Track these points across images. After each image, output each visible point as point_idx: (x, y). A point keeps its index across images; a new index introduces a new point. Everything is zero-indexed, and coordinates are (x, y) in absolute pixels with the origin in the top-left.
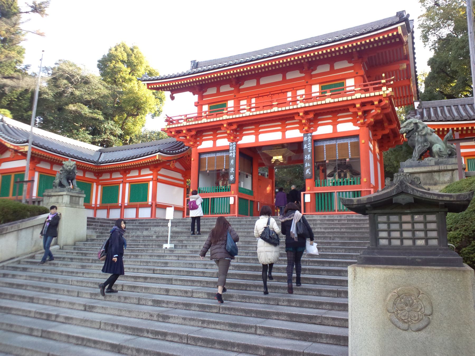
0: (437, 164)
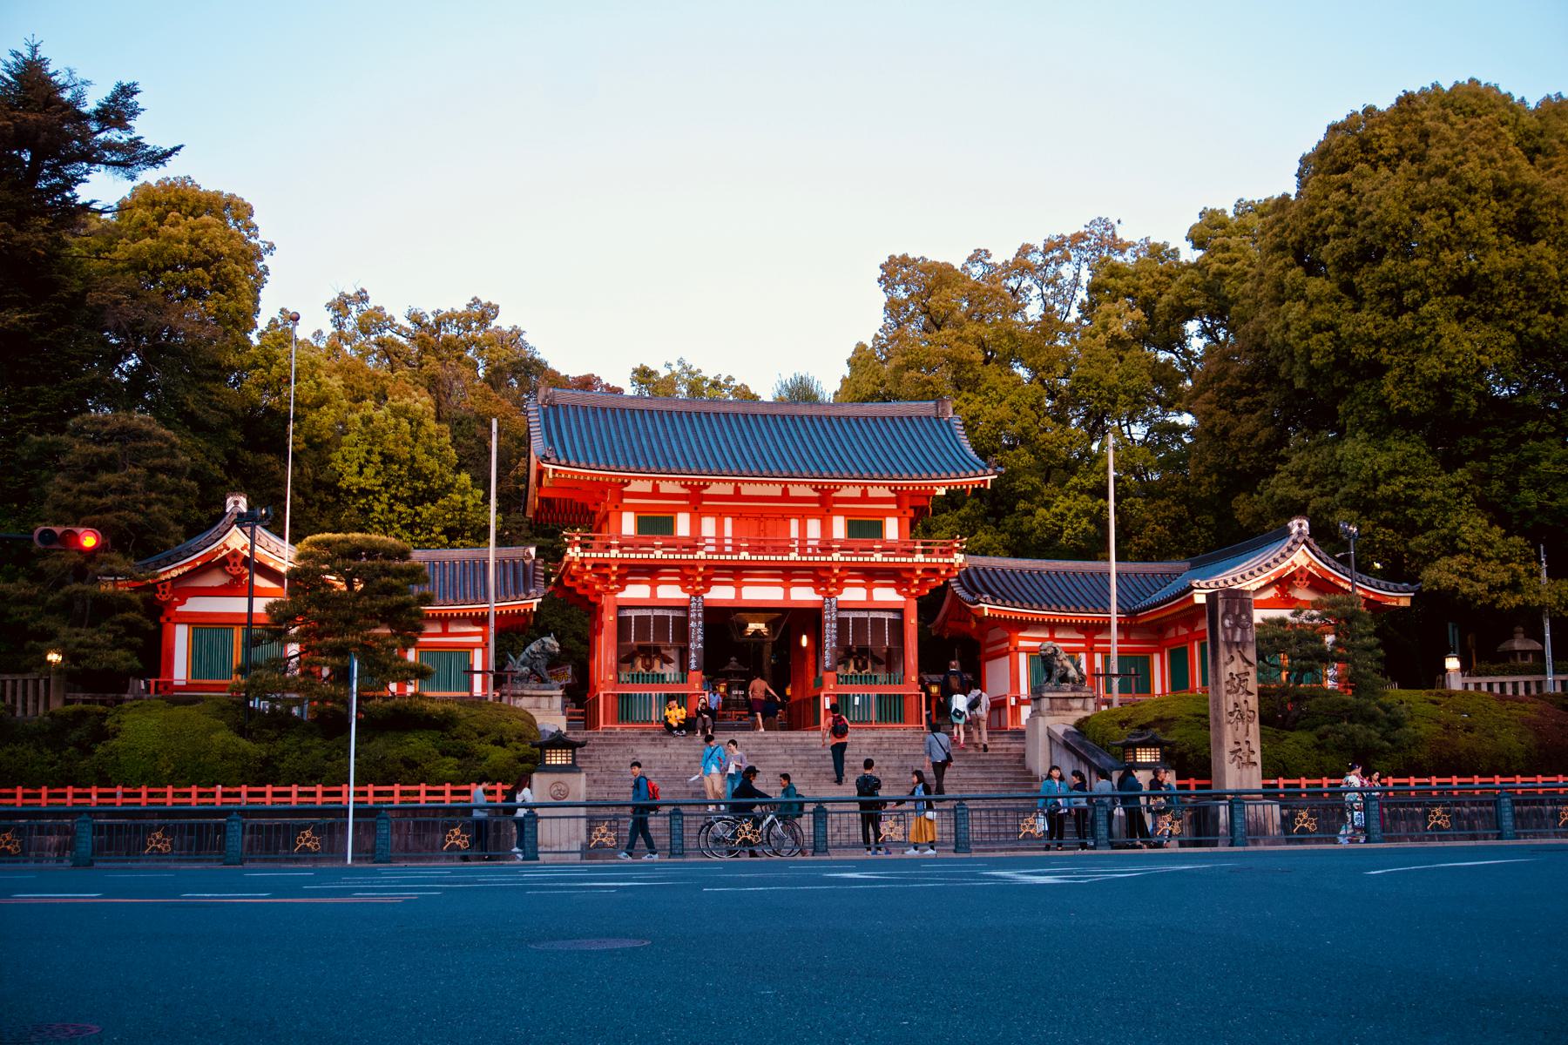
0: (1073, 690)
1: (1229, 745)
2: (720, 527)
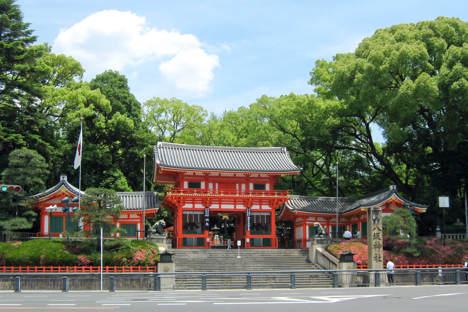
1: (373, 255)
2: (214, 187)
